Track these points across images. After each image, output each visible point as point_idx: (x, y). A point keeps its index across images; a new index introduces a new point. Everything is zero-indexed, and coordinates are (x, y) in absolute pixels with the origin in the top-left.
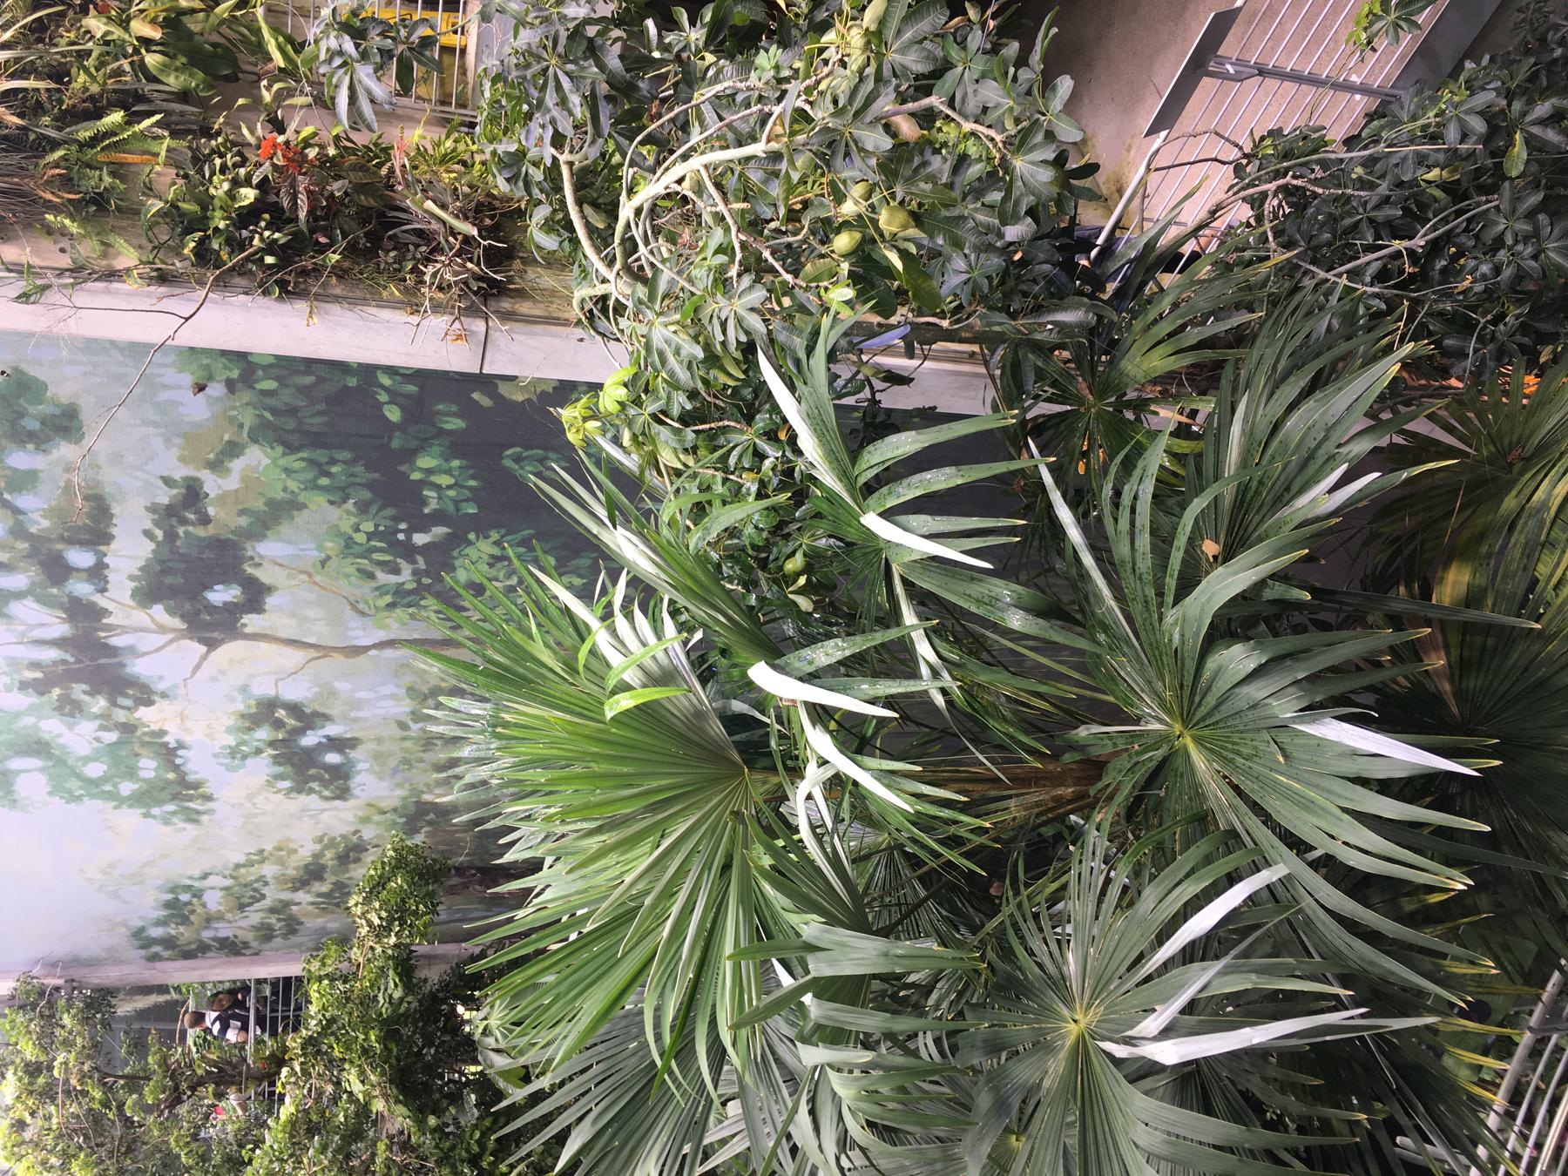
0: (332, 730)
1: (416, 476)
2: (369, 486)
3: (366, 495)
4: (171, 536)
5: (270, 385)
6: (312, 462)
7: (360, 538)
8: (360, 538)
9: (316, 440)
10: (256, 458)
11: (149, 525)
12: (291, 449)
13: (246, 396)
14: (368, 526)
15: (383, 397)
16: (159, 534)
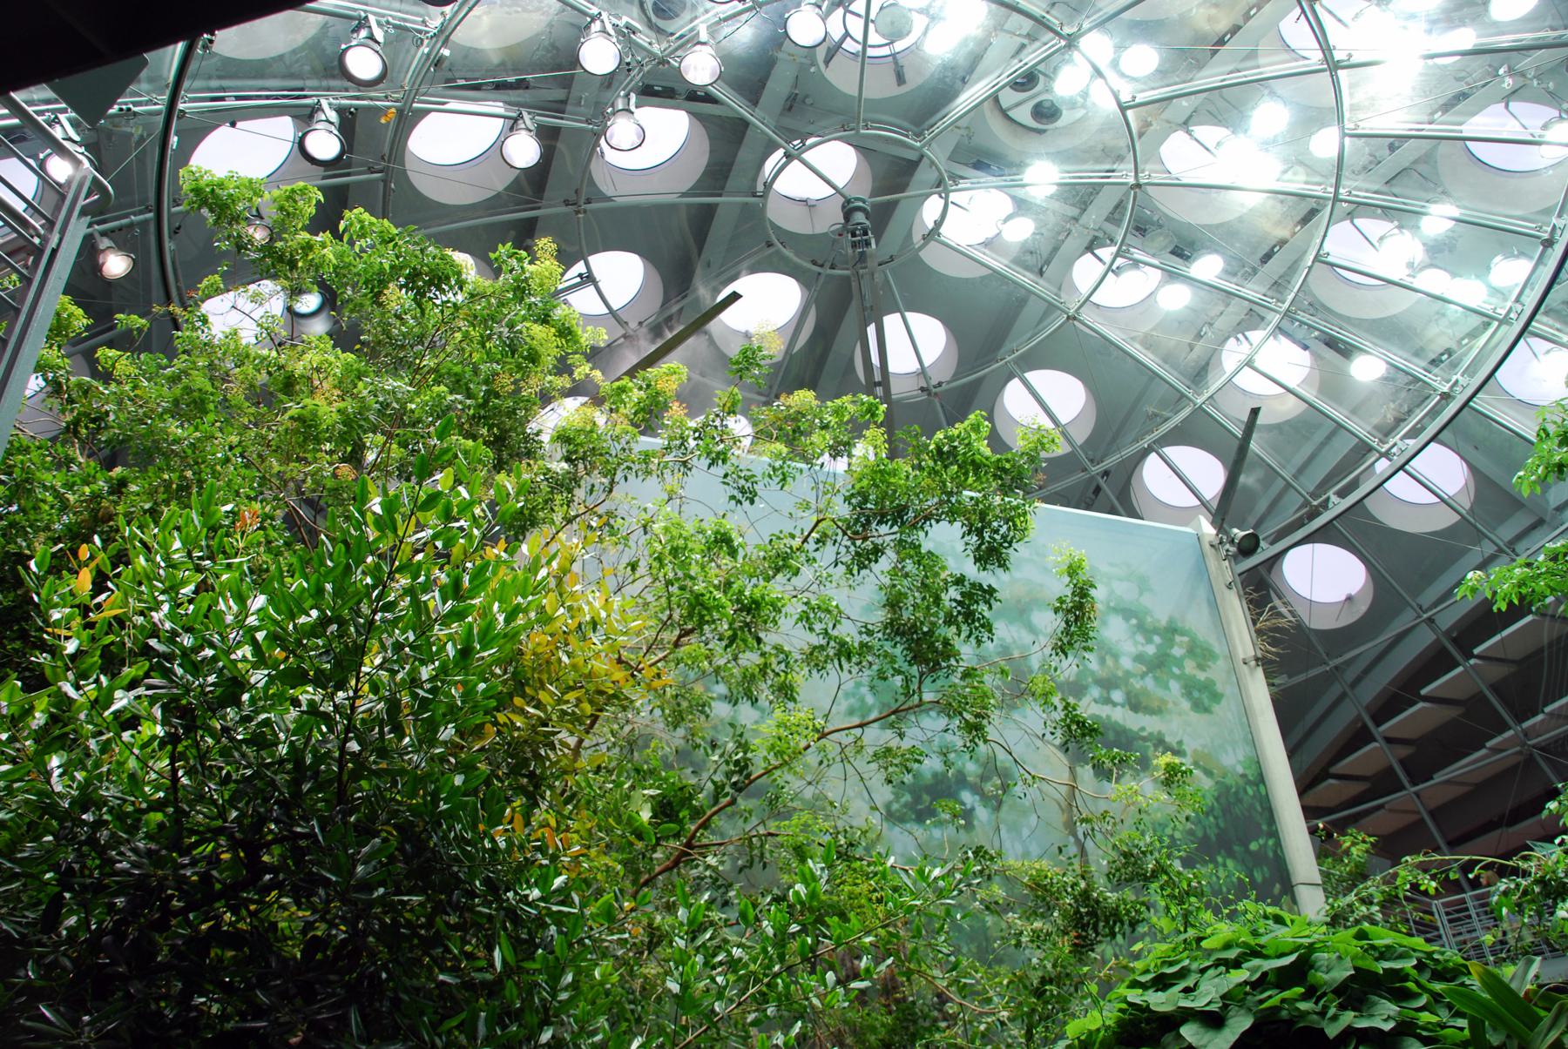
0: (982, 814)
1: (1220, 859)
2: (1206, 836)
3: (1200, 834)
4: (1144, 739)
5: (1250, 792)
6: (1212, 809)
7: (1169, 831)
8: (1169, 831)
9: (1226, 811)
10: (1207, 784)
11: (1149, 730)
12: (1217, 799)
13: (1241, 782)
14: (1177, 835)
15: (1261, 841)
16: (1144, 734)
